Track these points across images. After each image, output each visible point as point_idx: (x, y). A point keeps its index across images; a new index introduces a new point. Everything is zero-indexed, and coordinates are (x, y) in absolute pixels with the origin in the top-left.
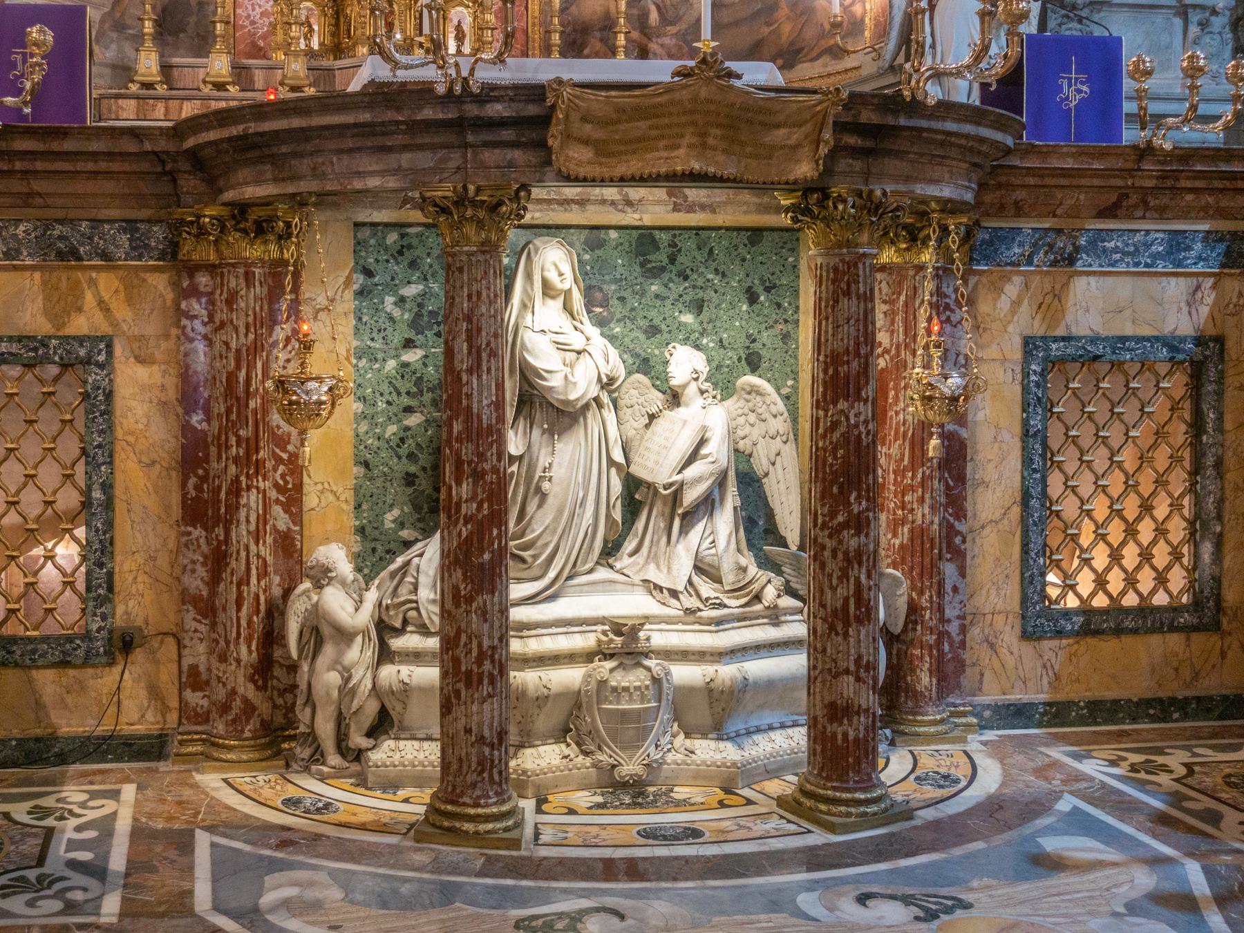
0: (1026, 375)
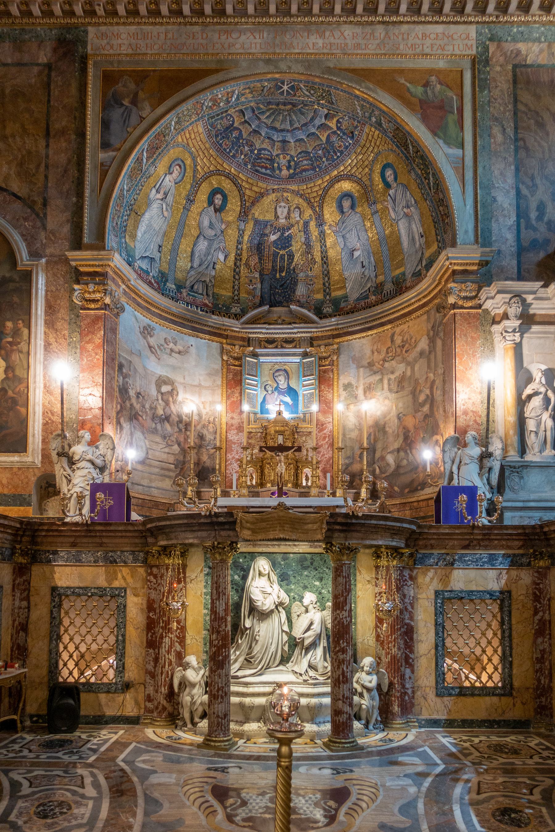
0: (436, 603)
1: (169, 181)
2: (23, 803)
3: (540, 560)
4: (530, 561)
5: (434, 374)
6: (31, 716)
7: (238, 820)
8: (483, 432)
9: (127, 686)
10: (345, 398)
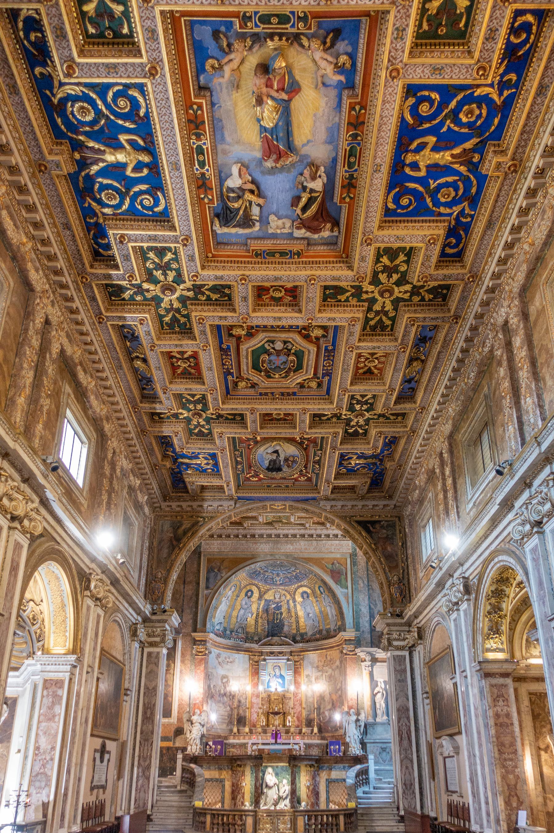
1: (230, 593)
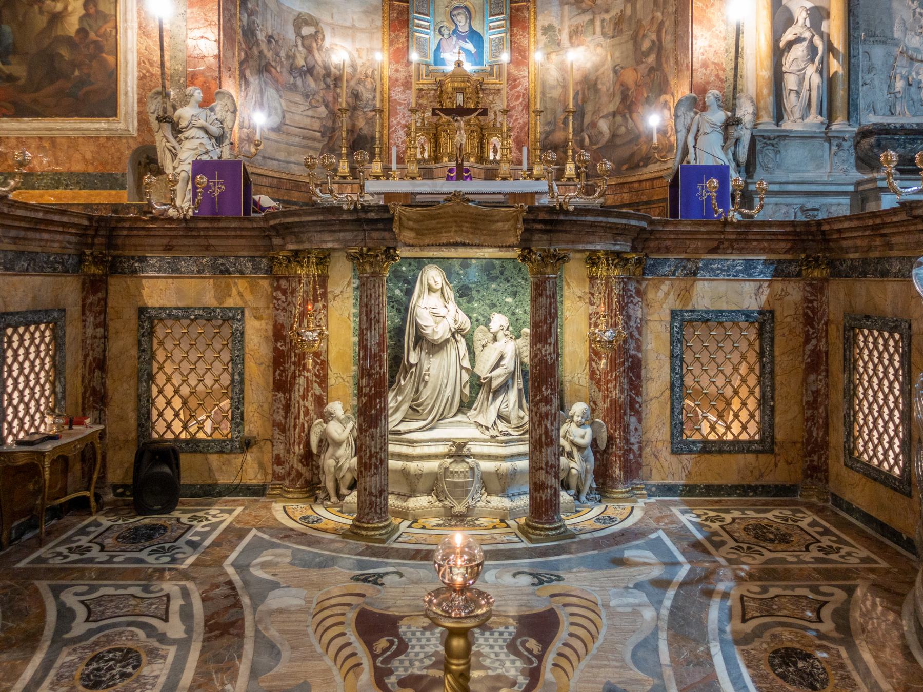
2: (69, 654)
3: (815, 268)
4: (801, 270)
5: (663, 14)
6: (115, 487)
7: (392, 684)
8: (729, 91)
9: (247, 444)
10: (545, 44)
